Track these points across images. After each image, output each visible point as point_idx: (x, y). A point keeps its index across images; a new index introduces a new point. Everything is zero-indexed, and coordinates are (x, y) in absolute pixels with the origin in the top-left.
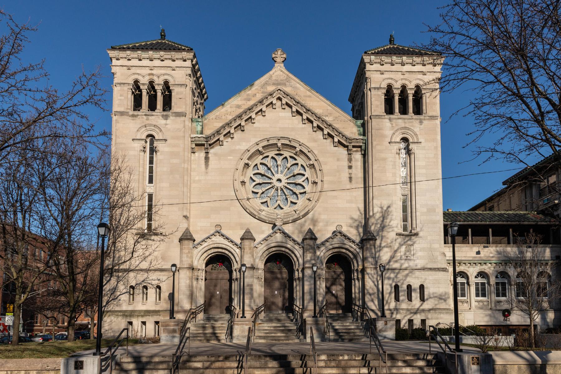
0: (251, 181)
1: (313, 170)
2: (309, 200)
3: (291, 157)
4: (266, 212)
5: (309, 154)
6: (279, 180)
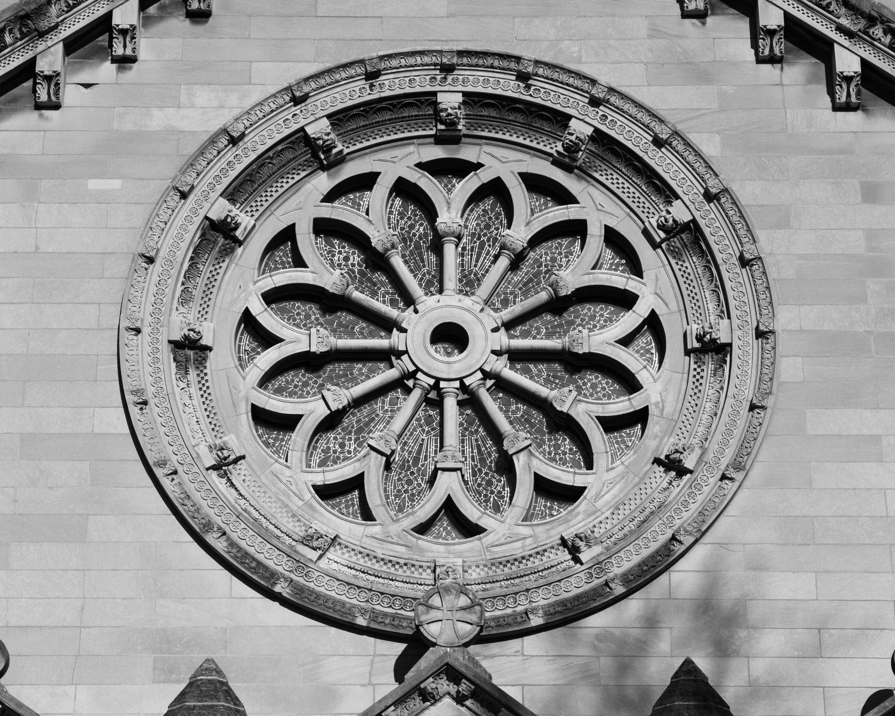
0: (246, 341)
1: (693, 264)
2: (673, 465)
3: (535, 184)
4: (358, 551)
5: (662, 163)
6: (451, 336)
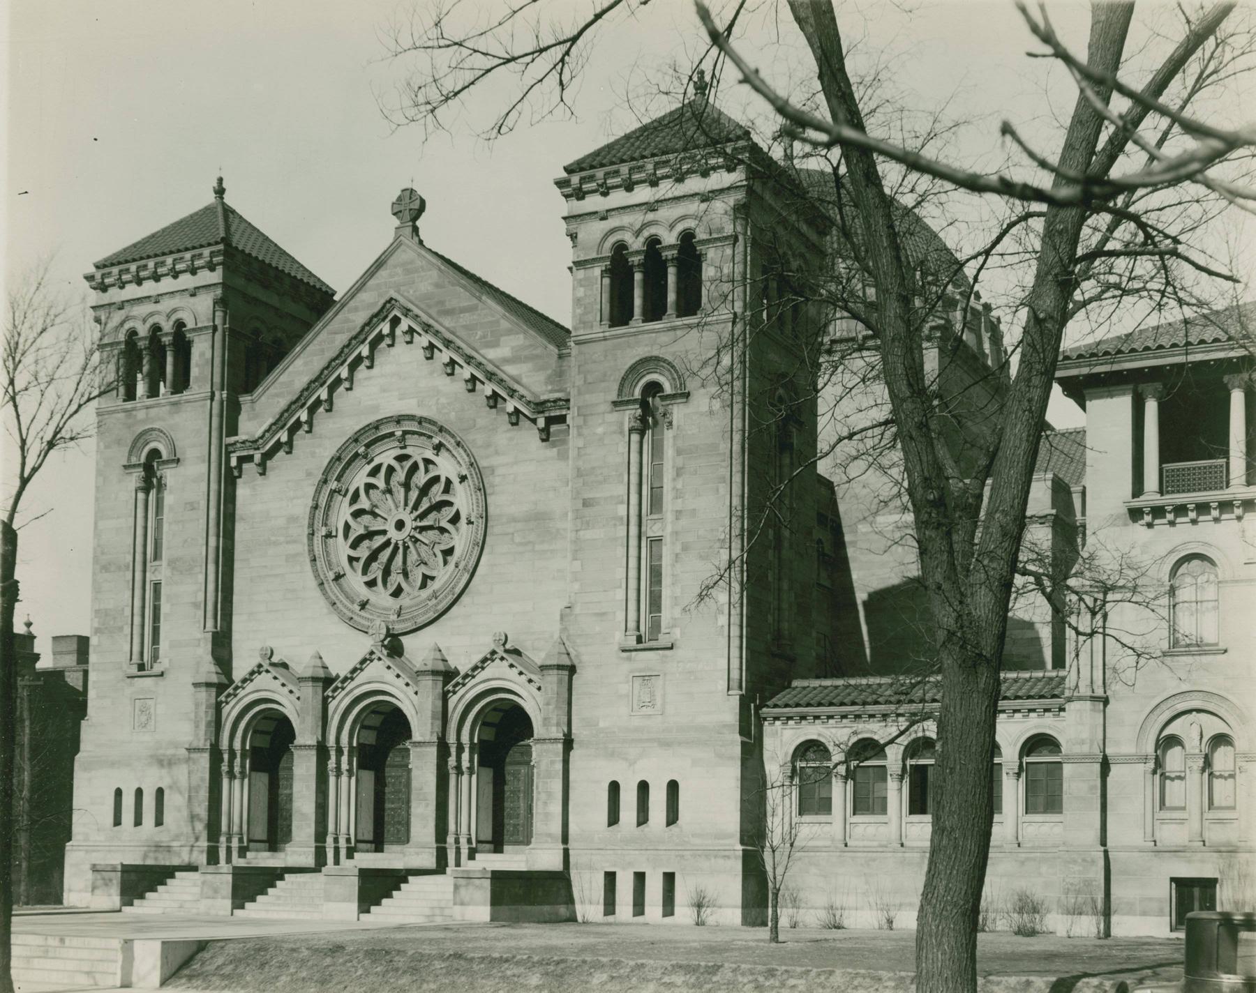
5: (384, 430)
6: (400, 525)
